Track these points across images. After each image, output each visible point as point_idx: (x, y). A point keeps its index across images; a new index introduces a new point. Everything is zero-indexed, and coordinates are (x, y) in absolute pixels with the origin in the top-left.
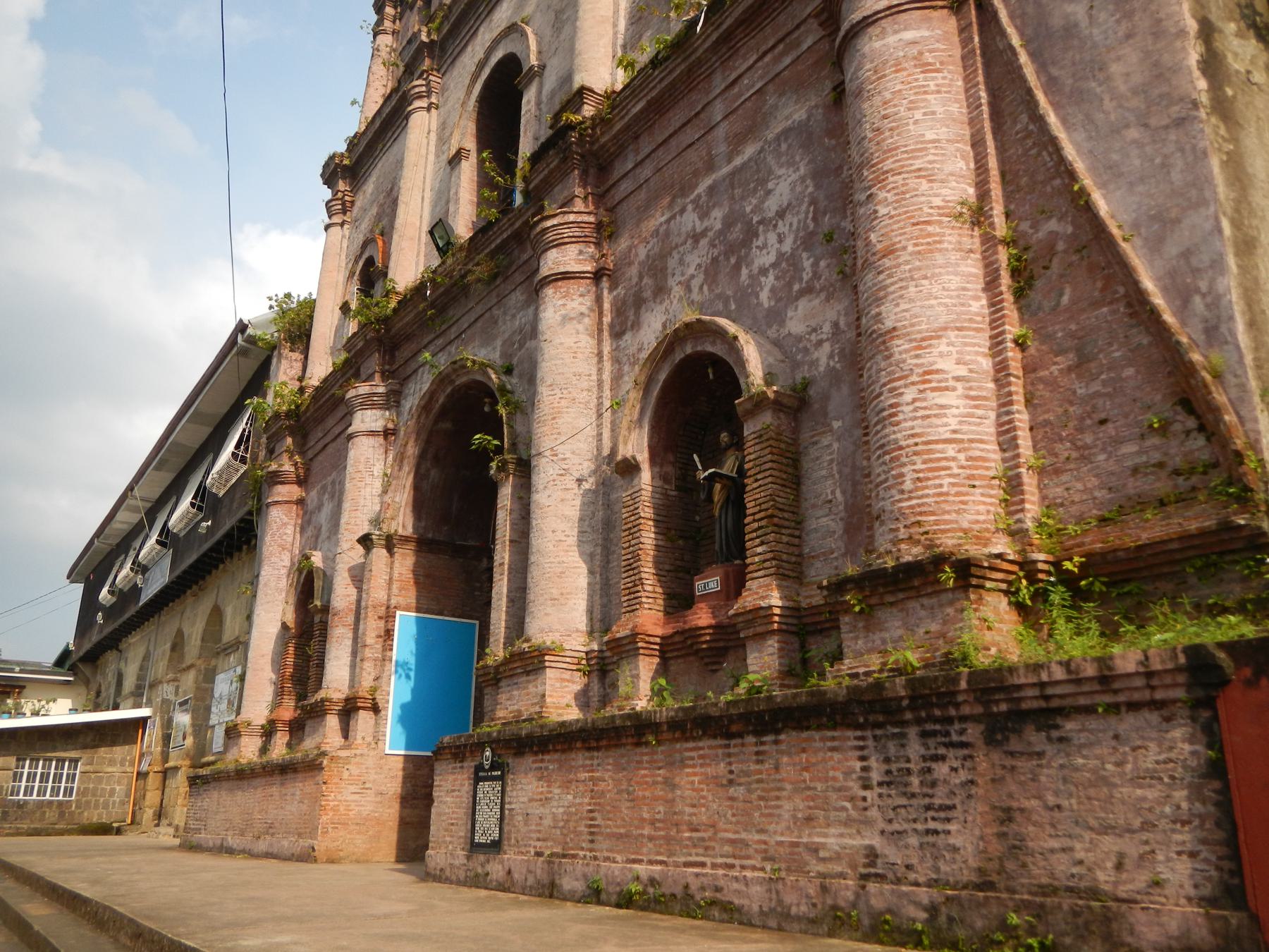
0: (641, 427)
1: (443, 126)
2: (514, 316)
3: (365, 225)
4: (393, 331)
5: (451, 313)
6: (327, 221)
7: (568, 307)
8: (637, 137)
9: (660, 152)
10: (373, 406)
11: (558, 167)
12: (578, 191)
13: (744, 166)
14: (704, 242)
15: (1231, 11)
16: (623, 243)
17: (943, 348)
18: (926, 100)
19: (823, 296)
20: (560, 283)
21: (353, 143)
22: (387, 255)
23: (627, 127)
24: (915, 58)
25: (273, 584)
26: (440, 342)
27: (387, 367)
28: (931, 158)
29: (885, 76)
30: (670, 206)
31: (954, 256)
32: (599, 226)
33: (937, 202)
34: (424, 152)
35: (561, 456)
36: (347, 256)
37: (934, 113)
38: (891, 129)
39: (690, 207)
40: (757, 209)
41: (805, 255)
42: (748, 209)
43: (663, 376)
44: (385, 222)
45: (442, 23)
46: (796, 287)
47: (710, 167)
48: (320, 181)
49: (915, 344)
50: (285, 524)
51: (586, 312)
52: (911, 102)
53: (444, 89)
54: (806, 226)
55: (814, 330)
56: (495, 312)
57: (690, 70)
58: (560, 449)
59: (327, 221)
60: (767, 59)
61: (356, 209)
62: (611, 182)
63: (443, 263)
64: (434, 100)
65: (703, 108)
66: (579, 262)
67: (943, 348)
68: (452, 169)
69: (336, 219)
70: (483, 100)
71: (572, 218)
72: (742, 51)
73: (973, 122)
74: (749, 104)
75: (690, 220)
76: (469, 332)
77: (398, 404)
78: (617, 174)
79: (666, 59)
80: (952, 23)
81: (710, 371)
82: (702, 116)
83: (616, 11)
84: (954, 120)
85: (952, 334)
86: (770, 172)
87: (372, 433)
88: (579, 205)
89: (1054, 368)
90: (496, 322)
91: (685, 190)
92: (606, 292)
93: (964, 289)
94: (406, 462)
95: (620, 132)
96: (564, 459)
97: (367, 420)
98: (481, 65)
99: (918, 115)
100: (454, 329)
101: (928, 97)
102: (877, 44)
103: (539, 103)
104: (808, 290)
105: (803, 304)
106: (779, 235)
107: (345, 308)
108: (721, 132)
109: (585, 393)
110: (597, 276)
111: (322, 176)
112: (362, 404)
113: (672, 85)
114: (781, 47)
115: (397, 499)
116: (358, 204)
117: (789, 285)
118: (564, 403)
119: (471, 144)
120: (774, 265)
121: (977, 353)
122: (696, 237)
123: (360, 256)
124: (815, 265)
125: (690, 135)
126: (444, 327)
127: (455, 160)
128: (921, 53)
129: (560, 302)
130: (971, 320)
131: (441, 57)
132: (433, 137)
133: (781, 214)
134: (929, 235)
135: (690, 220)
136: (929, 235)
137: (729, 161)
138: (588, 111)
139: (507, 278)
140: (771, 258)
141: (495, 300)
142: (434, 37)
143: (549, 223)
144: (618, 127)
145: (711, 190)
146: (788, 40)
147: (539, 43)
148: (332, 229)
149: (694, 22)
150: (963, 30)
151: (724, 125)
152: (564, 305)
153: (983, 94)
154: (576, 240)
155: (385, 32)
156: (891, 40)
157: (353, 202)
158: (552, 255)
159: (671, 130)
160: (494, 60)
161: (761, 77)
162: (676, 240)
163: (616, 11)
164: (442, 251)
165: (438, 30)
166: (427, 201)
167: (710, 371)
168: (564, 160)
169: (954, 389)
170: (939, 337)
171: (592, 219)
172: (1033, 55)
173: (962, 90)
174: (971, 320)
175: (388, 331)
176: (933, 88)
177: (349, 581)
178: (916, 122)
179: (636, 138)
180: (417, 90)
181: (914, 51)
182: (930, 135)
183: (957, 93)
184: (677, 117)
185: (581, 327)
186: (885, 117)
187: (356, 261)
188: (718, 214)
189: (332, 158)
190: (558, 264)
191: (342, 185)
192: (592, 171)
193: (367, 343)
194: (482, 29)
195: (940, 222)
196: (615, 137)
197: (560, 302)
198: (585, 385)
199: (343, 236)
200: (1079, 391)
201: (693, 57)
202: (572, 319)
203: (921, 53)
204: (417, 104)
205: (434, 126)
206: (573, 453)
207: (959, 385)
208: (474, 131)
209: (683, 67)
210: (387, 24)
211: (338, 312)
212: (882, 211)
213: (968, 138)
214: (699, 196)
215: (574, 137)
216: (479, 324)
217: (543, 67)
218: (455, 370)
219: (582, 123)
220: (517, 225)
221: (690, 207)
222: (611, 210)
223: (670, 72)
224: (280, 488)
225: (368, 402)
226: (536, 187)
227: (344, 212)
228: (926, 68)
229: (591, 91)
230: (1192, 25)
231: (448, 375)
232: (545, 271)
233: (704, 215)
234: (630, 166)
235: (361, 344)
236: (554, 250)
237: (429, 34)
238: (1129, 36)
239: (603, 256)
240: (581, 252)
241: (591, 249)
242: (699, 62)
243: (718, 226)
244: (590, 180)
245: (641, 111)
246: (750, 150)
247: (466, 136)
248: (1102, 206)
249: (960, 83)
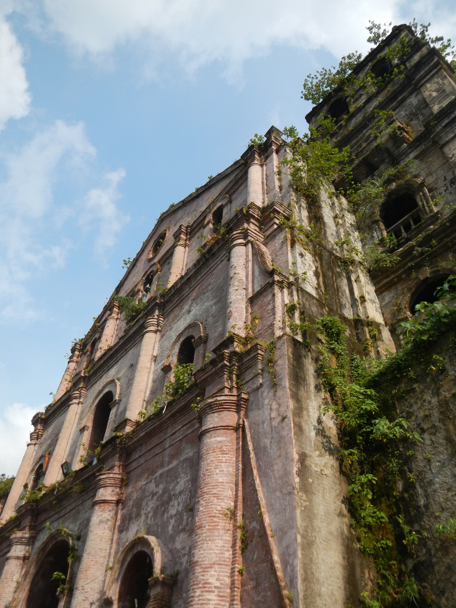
0: (117, 582)
1: (82, 412)
2: (86, 512)
3: (44, 447)
4: (39, 507)
5: (64, 503)
6: (29, 442)
7: (103, 516)
8: (141, 445)
9: (148, 453)
10: (22, 544)
12: (117, 463)
13: (172, 468)
14: (155, 498)
15: (318, 447)
16: (130, 489)
17: (212, 573)
18: (221, 465)
19: (188, 533)
20: (102, 504)
21: (48, 408)
22: (48, 463)
23: (138, 441)
24: (220, 448)
26: (57, 516)
27: (33, 524)
28: (219, 489)
29: (209, 453)
30: (147, 478)
31: (222, 532)
32: (122, 480)
33: (219, 508)
34: (72, 422)
35: (86, 590)
36: (34, 460)
37: (223, 471)
38: (208, 475)
39: (153, 481)
40: (173, 489)
42: (171, 488)
43: (129, 559)
44: (51, 449)
45: (90, 369)
46: (181, 527)
47: (162, 466)
48: (31, 423)
49: (203, 570)
51: (110, 519)
52: (216, 465)
53: (86, 397)
56: (80, 508)
57: (161, 425)
58: (86, 587)
59: (29, 442)
60: (185, 428)
61: (42, 438)
62: (130, 461)
63: (64, 480)
64: (81, 400)
66: (111, 495)
67: (212, 573)
68: (81, 433)
69: (33, 442)
70: (98, 406)
71: (111, 475)
72: (178, 422)
73: (237, 475)
74: (177, 444)
75: (152, 486)
76: (68, 515)
77: (33, 543)
78: (133, 458)
79: (153, 419)
80: (235, 435)
82: (163, 443)
83: (146, 388)
84: (230, 474)
85: (216, 566)
86: (179, 475)
87: (18, 558)
88: (116, 470)
89: (249, 586)
90: (79, 513)
91: (153, 472)
92: (119, 511)
93: (224, 547)
94: (28, 576)
95: (135, 442)
96: (87, 592)
98: (100, 392)
99: (218, 471)
100: (63, 511)
101: (222, 464)
102: (209, 440)
103: (116, 415)
106: (178, 502)
107: (26, 486)
108: (167, 452)
109: (102, 559)
110: (118, 502)
111: (32, 421)
113: (154, 429)
114: (189, 425)
115: (20, 596)
116: (44, 436)
117: (178, 526)
118: (92, 563)
119: (90, 424)
120: (175, 515)
121: (225, 576)
123: (38, 462)
125: (158, 450)
126: (60, 509)
127: (82, 430)
128: (222, 446)
129: (100, 513)
130: (224, 561)
131: (88, 382)
132: (78, 416)
133: (180, 493)
134: (214, 522)
135: (152, 486)
136: (214, 522)
137: (168, 465)
138: (128, 429)
139: (87, 493)
141: (81, 502)
142: (87, 375)
143: (102, 477)
144: (135, 440)
145: (161, 475)
147: (121, 390)
148: (30, 446)
149: (162, 409)
150: (238, 438)
151: (169, 449)
152: (101, 515)
153: (240, 465)
154: (112, 485)
155: (73, 361)
156: (213, 440)
157: (42, 435)
158: (101, 491)
159: (152, 446)
160: (105, 392)
161: (182, 435)
162: (147, 494)
163: (146, 388)
164: (65, 475)
165: (89, 372)
166: (69, 444)
168: (113, 449)
169: (214, 592)
170: (211, 568)
171: (120, 477)
172: (256, 454)
173: (234, 462)
174: (224, 561)
175: (37, 506)
176: (224, 461)
178: (217, 474)
179: (141, 445)
181: (220, 445)
182: (220, 480)
183: (233, 463)
184: (155, 441)
185: (106, 526)
186: (207, 470)
187: (36, 465)
188: (161, 486)
189: (38, 414)
190: (102, 495)
191: (39, 427)
192: (124, 455)
193: (27, 511)
194: (104, 376)
195: (219, 517)
196: (134, 443)
197: (100, 513)
198: (103, 554)
199: (34, 450)
200: (256, 599)
201: (162, 420)
202: (103, 522)
203: (222, 446)
204: (75, 401)
205: (79, 411)
206: (91, 589)
207: (216, 590)
208: (93, 418)
209: (158, 423)
210: (75, 358)
211: (22, 488)
212: (201, 509)
213: (234, 481)
214: (157, 477)
215: (118, 441)
216: (73, 512)
217: (120, 400)
219: (121, 436)
221: (153, 481)
222: (128, 473)
223: (154, 424)
225: (20, 541)
226: (102, 458)
227: (37, 438)
228: (223, 452)
229: (130, 420)
230: (296, 457)
232: (97, 499)
233: (157, 486)
234: (137, 457)
235: (24, 511)
236: (102, 489)
237: (85, 373)
238: (280, 456)
239: (121, 494)
240: (113, 491)
241: (117, 490)
242: (164, 422)
243: (161, 492)
244: (123, 459)
245: (143, 436)
246: (175, 463)
247: (89, 422)
248: (267, 520)
249: (234, 459)
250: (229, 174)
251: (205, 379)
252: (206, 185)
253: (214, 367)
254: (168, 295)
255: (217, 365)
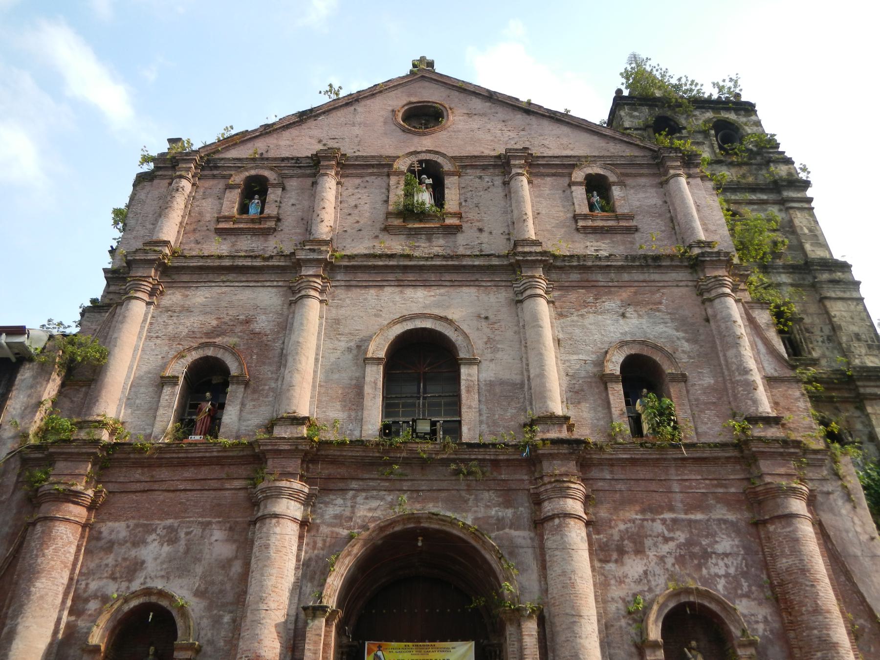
10: (297, 500)
11: (565, 454)
19: (756, 602)
25: (50, 599)
41: (743, 580)
46: (739, 592)
50: (70, 543)
54: (742, 568)
55: (753, 615)
57: (657, 459)
65: (665, 480)
81: (688, 609)
87: (294, 520)
97: (291, 508)
104: (747, 596)
105: (745, 601)
112: (290, 495)
117: (735, 589)
122: (483, 473)
124: (749, 586)
140: (722, 572)
143: (573, 486)
146: (720, 481)
167: (688, 609)
168: (570, 454)
177: (275, 635)
180: (316, 285)
218: (429, 518)
220: (501, 457)
224: (72, 507)
225: (294, 495)
231: (419, 518)
242: (665, 459)
250: (605, 135)
251: (763, 452)
252: (555, 113)
253: (782, 447)
254: (564, 261)
255: (788, 448)
